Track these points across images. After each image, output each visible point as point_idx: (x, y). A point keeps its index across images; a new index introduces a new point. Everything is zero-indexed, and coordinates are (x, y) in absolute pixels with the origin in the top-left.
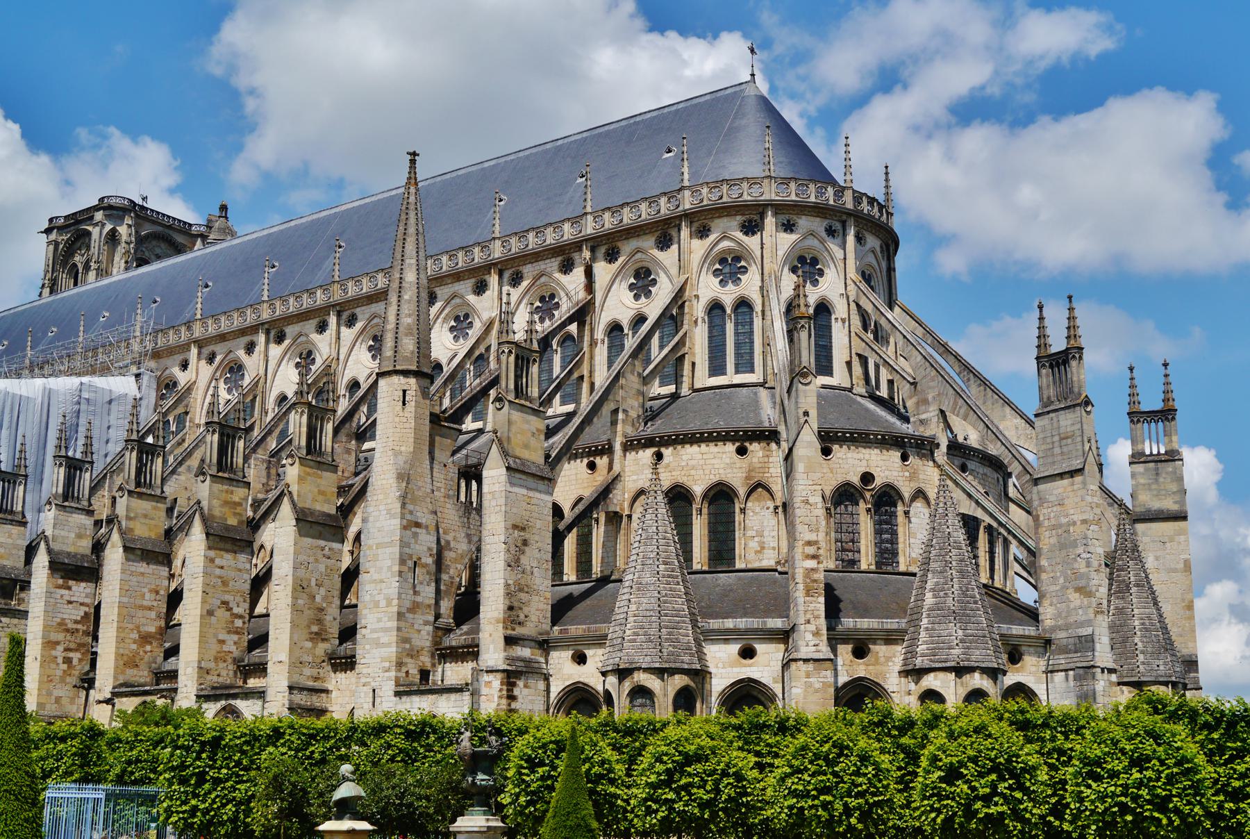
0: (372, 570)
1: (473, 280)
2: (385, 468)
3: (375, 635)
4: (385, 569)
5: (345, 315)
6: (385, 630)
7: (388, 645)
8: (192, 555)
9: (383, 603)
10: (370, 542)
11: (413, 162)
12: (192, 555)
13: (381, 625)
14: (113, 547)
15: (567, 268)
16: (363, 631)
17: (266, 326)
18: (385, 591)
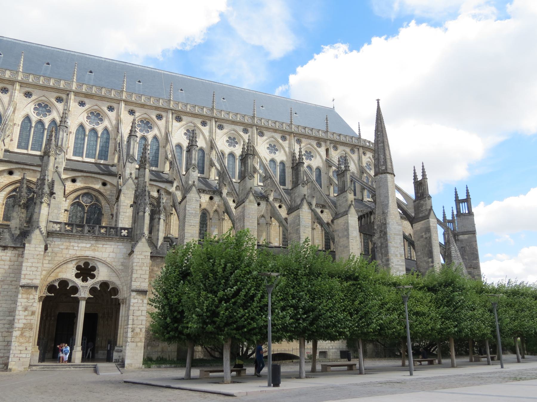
0: (393, 243)
1: (281, 135)
2: (394, 207)
3: (397, 267)
4: (398, 243)
5: (218, 124)
6: (400, 265)
7: (403, 271)
8: (304, 217)
9: (399, 255)
10: (391, 232)
11: (378, 103)
12: (304, 217)
13: (399, 263)
14: (250, 201)
15: (319, 145)
16: (392, 264)
17: (173, 111)
18: (399, 251)
